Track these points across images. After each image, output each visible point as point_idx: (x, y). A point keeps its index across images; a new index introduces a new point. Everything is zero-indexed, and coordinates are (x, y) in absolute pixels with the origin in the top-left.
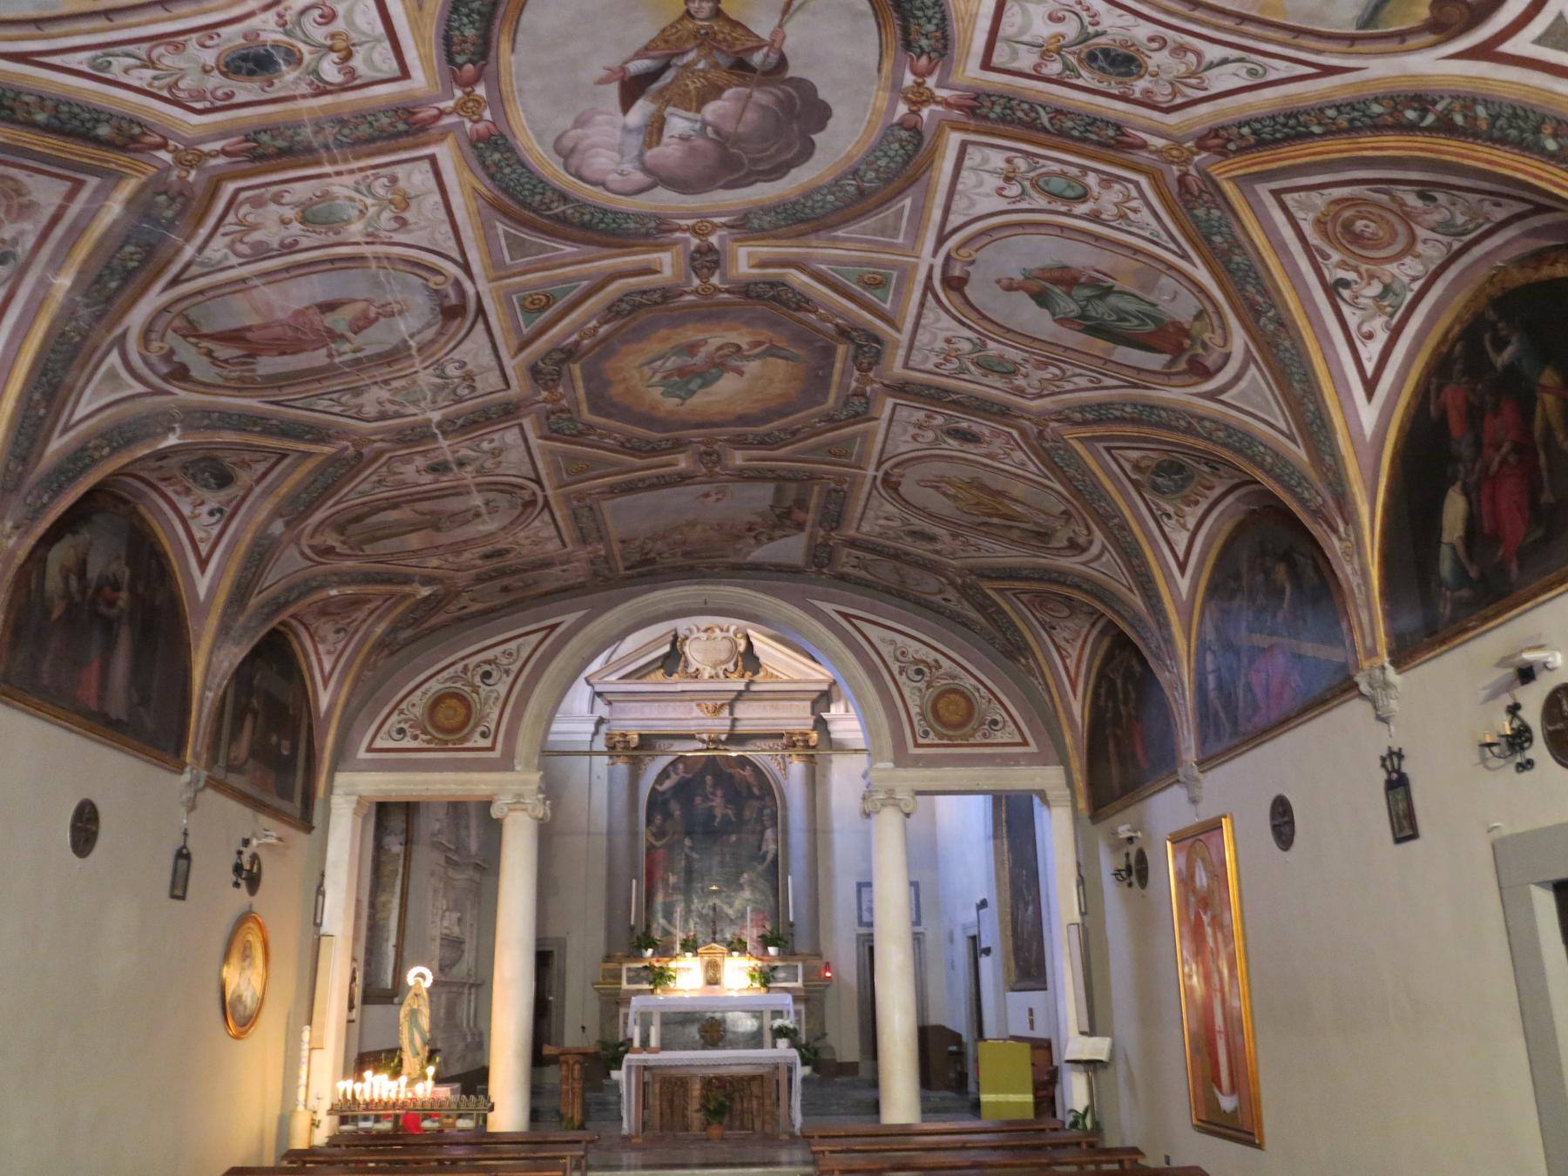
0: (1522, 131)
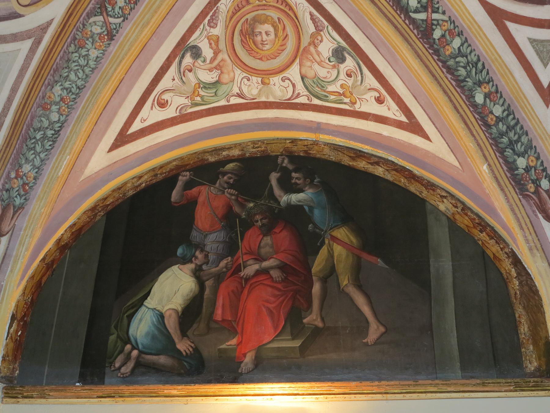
0: (468, 75)
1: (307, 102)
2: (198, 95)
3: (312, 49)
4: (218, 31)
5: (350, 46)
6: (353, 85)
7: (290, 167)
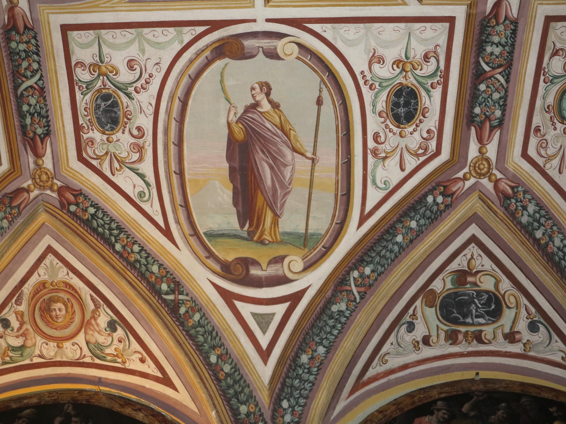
0: (205, 341)
1: (91, 361)
2: (8, 356)
3: (93, 321)
4: (23, 308)
5: (119, 319)
6: (123, 348)
7: (73, 413)
